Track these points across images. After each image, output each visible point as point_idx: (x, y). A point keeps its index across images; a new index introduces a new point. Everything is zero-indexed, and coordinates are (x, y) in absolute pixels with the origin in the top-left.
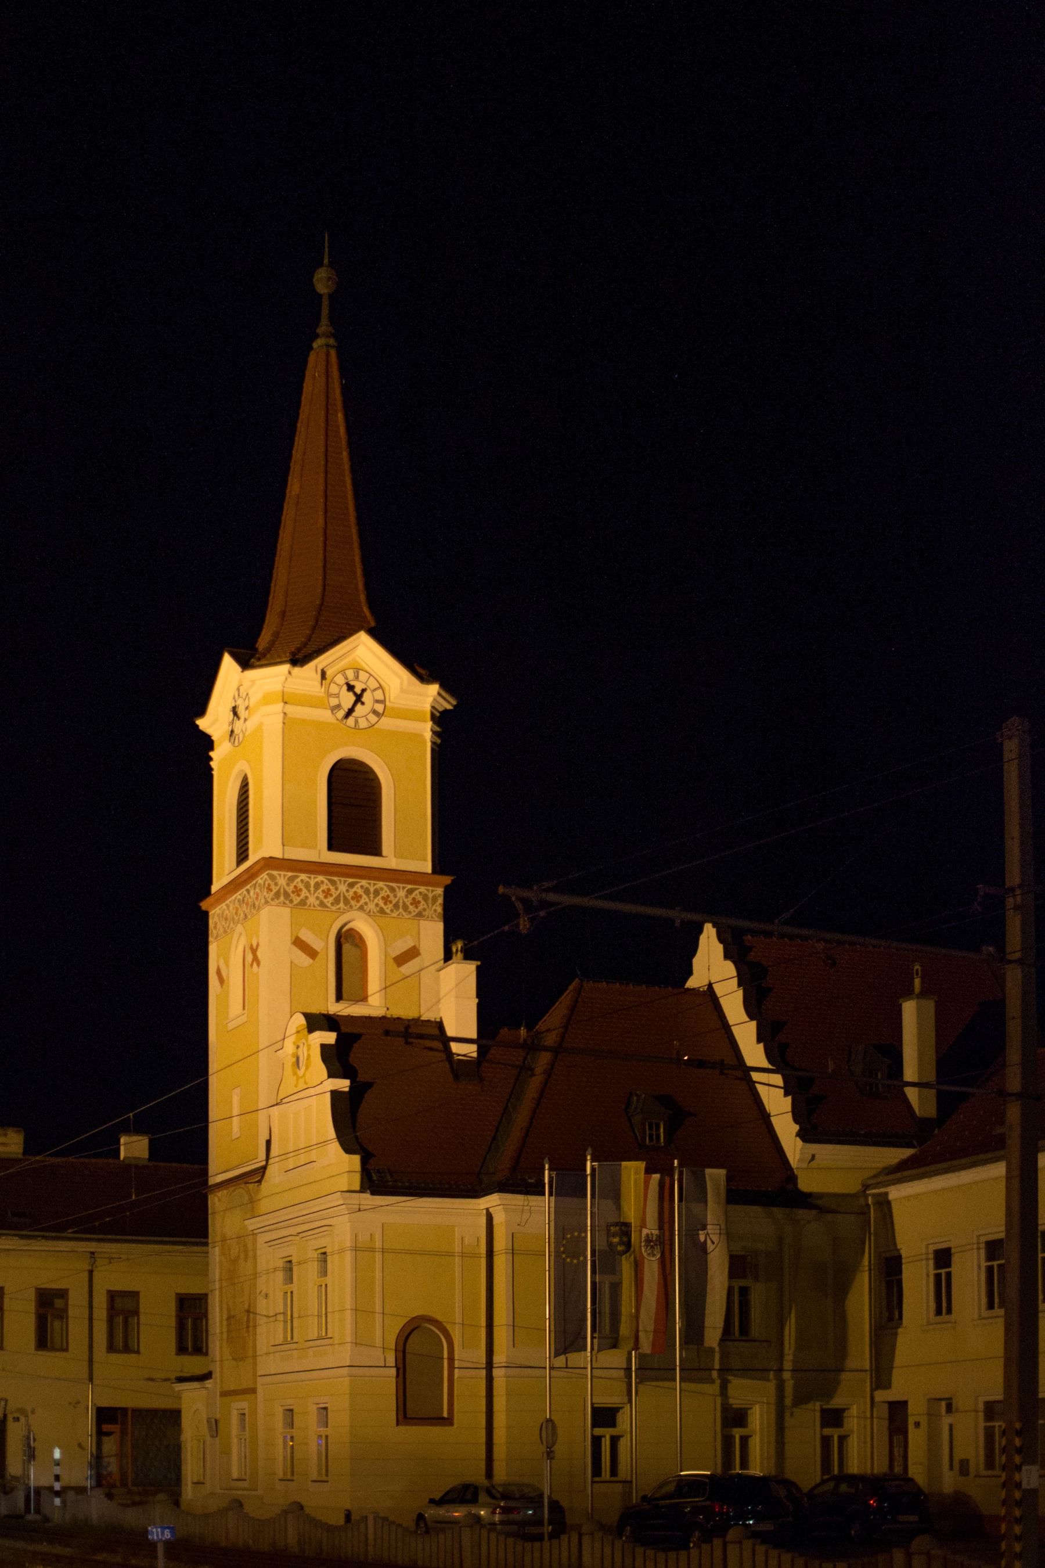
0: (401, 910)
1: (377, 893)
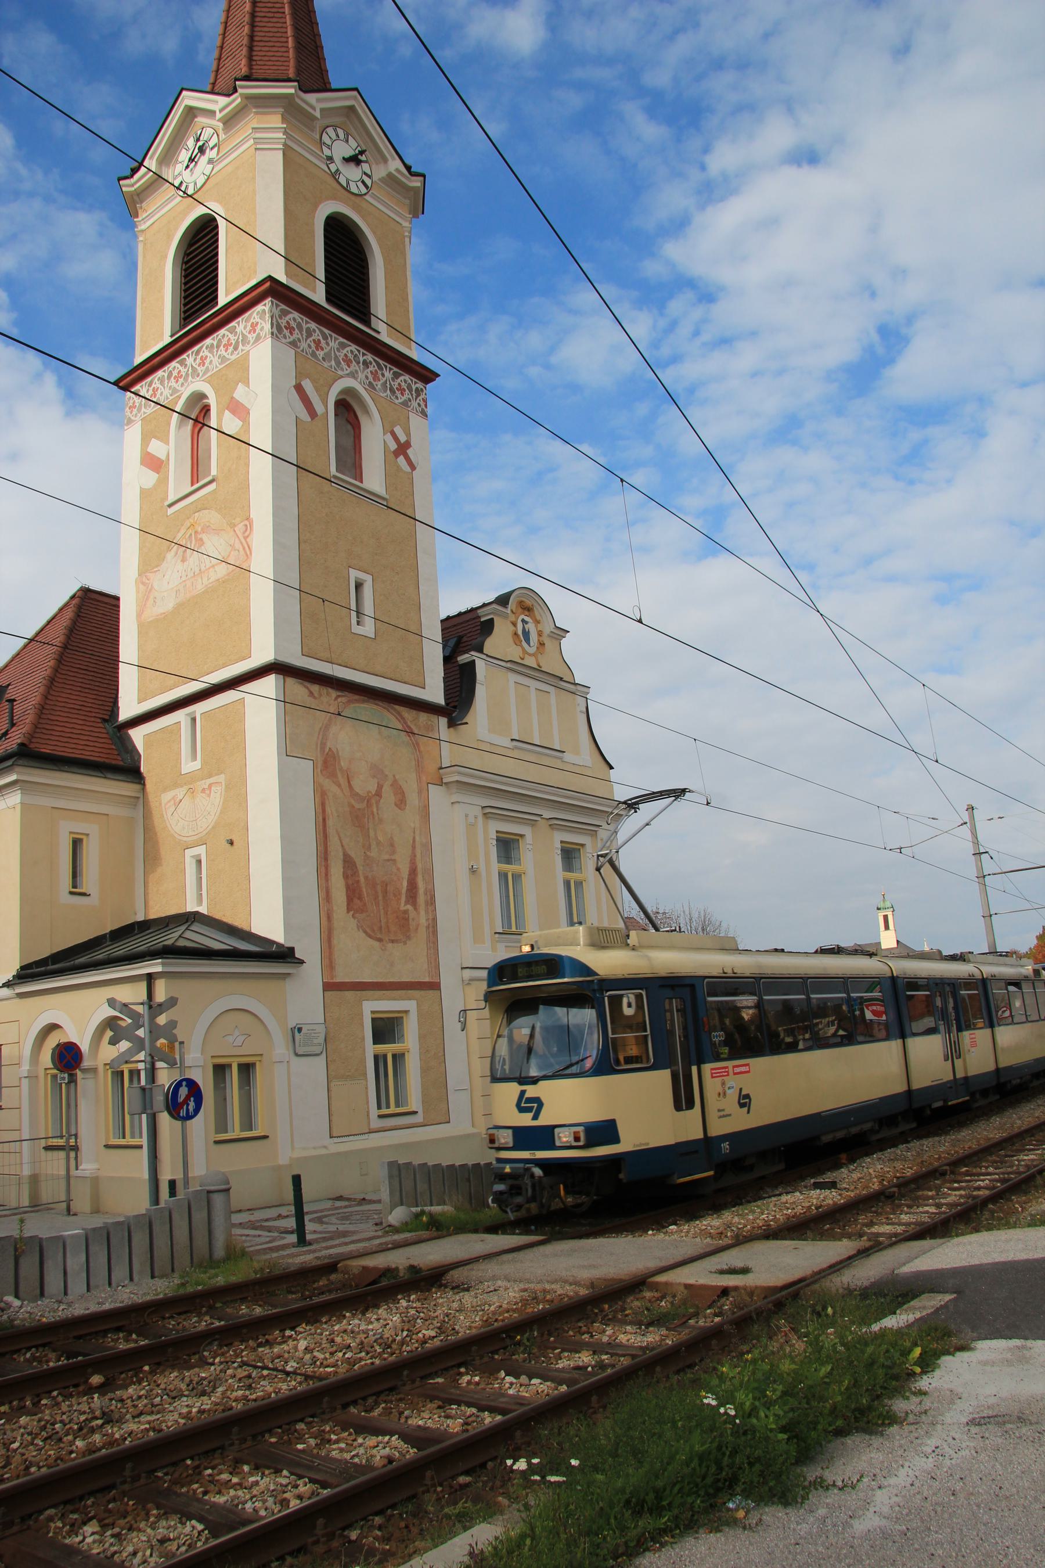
1: (366, 364)
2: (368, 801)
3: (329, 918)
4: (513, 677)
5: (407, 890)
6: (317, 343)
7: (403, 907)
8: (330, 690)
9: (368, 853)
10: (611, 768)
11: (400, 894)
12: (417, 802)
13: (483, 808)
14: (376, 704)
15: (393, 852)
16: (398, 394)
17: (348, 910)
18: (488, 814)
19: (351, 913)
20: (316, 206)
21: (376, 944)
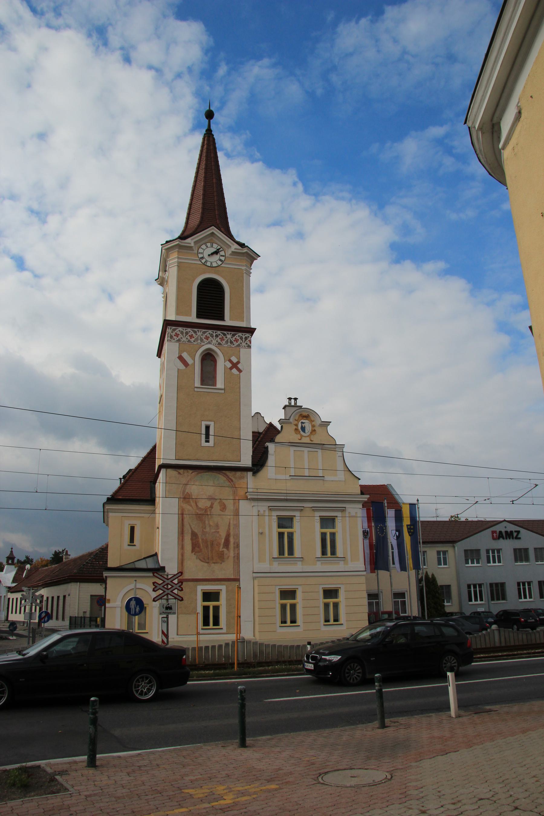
0: (229, 343)
1: (217, 336)
2: (205, 510)
3: (182, 555)
4: (292, 449)
5: (224, 543)
6: (191, 336)
7: (221, 550)
8: (189, 470)
9: (205, 530)
10: (359, 479)
11: (220, 544)
12: (232, 508)
13: (269, 507)
14: (213, 472)
15: (218, 528)
16: (235, 343)
17: (192, 552)
18: (271, 509)
19: (194, 553)
20: (194, 280)
21: (206, 564)
